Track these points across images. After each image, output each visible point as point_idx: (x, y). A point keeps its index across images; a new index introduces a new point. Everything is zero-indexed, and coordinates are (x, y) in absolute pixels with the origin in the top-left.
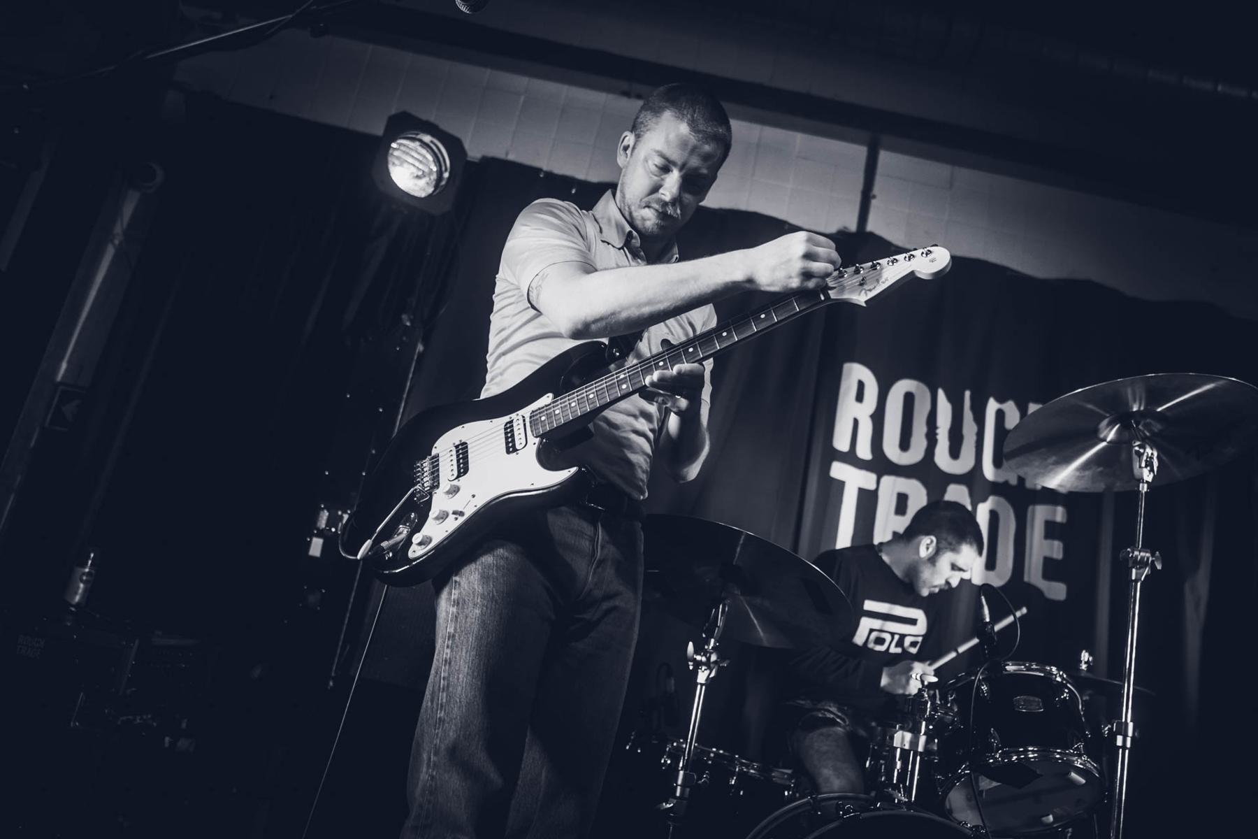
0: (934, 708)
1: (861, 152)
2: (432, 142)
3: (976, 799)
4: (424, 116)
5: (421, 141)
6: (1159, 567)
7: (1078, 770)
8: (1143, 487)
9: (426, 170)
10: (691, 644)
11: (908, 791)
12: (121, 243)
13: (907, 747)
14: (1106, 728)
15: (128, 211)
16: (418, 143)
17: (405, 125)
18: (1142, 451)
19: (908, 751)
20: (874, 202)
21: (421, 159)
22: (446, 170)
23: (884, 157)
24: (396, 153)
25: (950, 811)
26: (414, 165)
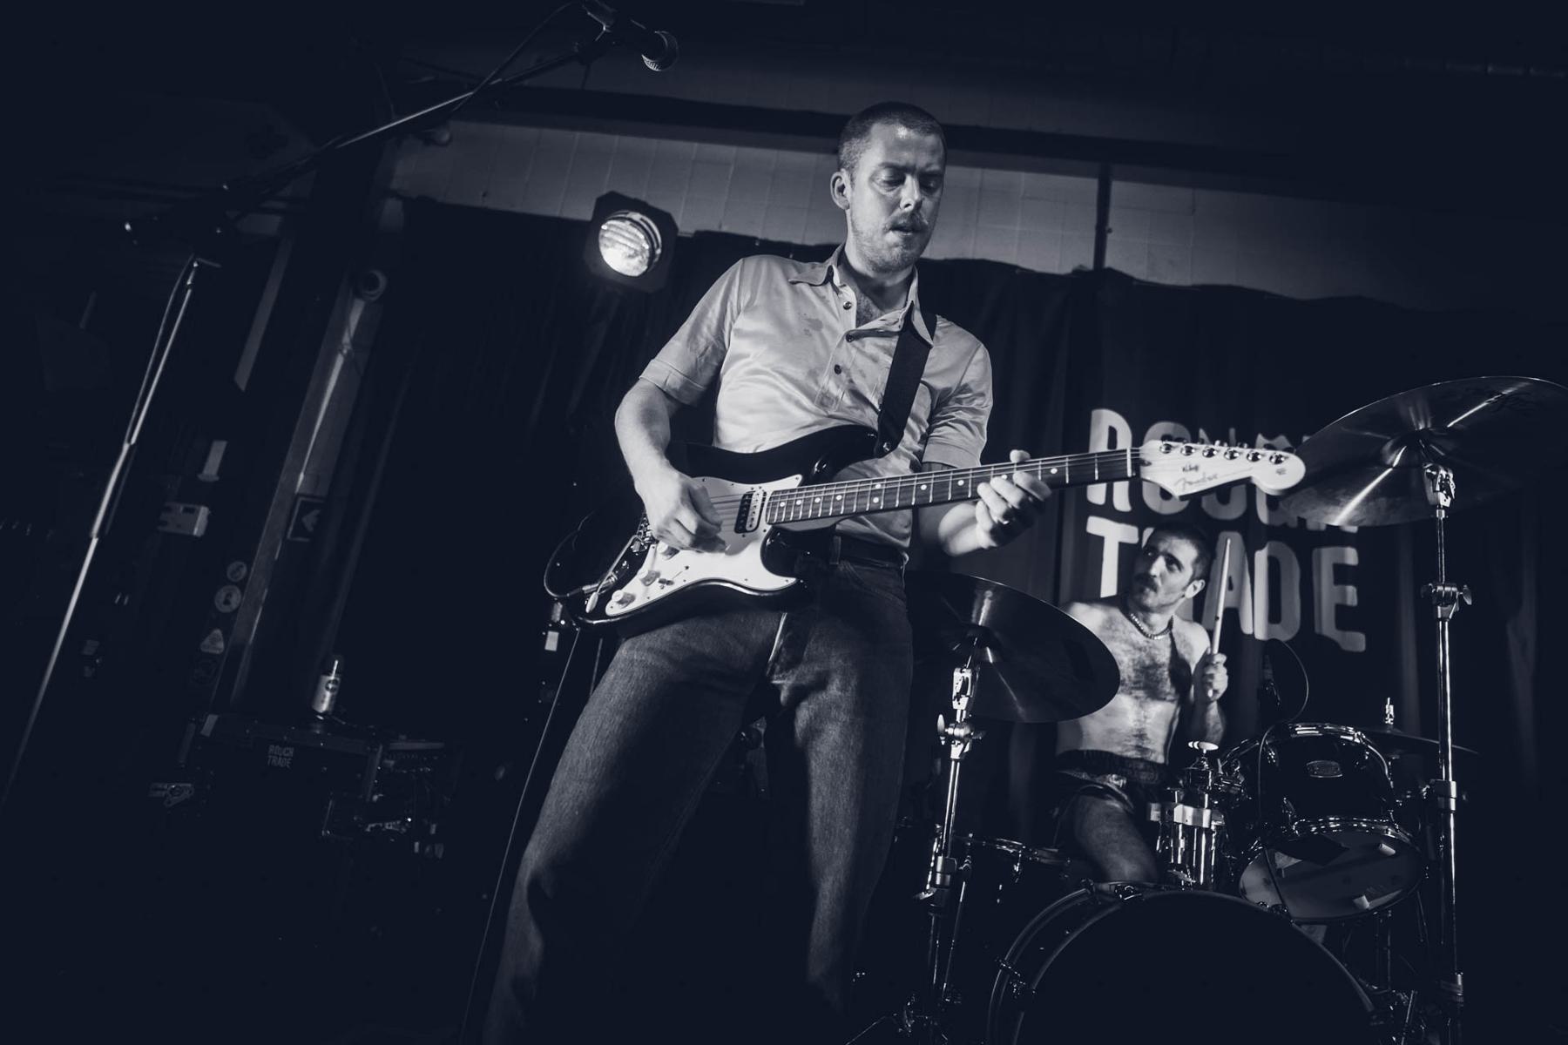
0: (1217, 780)
1: (1091, 185)
2: (642, 220)
3: (1274, 878)
4: (631, 194)
5: (630, 219)
6: (1469, 602)
7: (1389, 841)
8: (1440, 514)
9: (638, 249)
10: (941, 717)
11: (1196, 874)
12: (349, 352)
13: (1189, 823)
14: (1424, 790)
15: (354, 319)
16: (628, 223)
17: (612, 206)
18: (1434, 473)
19: (1192, 828)
20: (1110, 237)
21: (632, 237)
22: (658, 246)
23: (1117, 187)
24: (607, 235)
25: (1244, 892)
26: (626, 245)
